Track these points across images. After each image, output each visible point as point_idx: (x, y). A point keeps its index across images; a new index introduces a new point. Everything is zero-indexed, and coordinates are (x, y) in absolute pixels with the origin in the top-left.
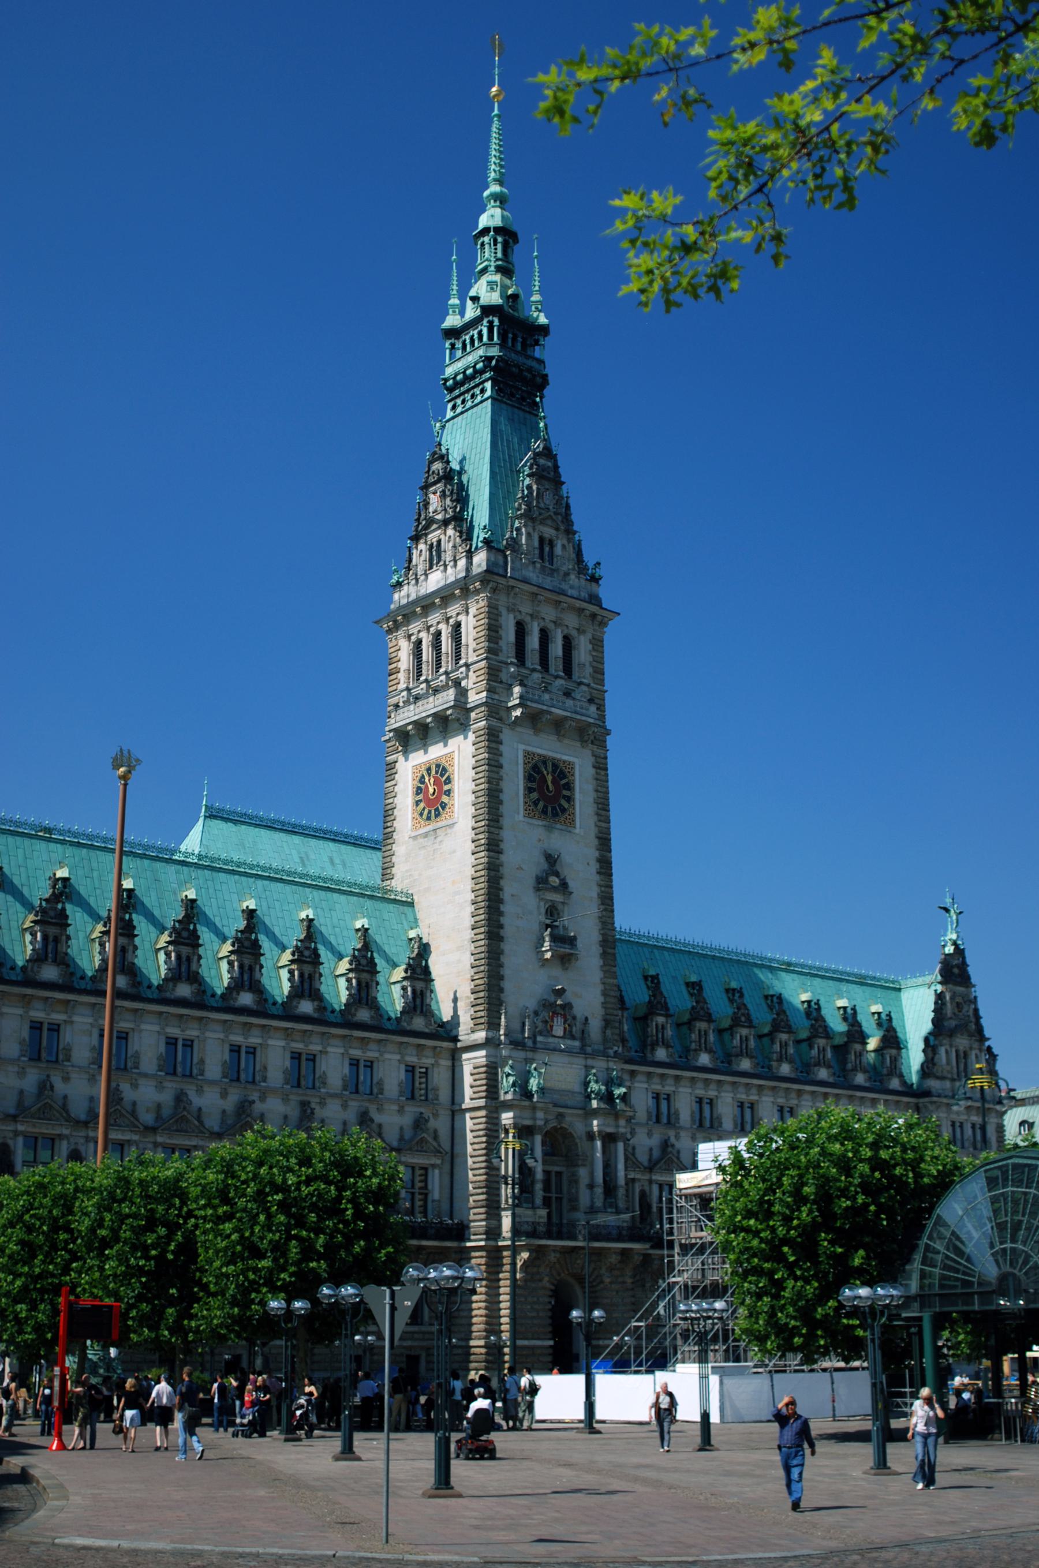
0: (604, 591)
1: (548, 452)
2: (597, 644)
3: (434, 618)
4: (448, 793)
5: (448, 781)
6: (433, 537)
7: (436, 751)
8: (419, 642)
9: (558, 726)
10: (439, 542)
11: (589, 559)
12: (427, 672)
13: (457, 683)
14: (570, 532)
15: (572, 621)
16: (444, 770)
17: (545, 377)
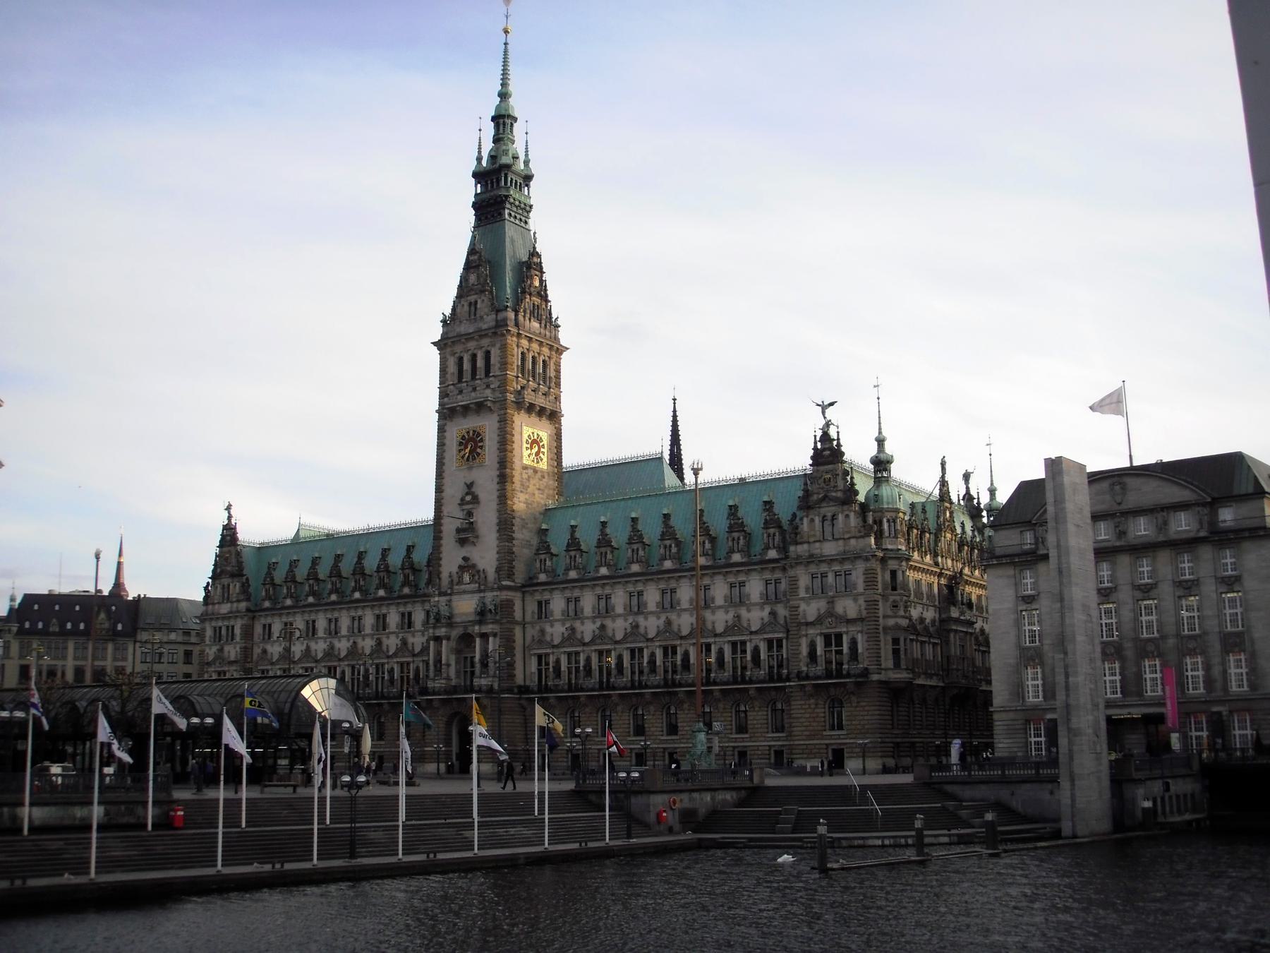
0: (561, 335)
1: (534, 254)
2: (558, 365)
3: (472, 345)
4: (481, 447)
5: (481, 440)
6: (472, 298)
7: (471, 423)
8: (461, 359)
9: (541, 412)
10: (476, 302)
11: (554, 316)
12: (467, 376)
13: (488, 386)
14: (547, 301)
15: (546, 350)
16: (479, 434)
17: (531, 207)
